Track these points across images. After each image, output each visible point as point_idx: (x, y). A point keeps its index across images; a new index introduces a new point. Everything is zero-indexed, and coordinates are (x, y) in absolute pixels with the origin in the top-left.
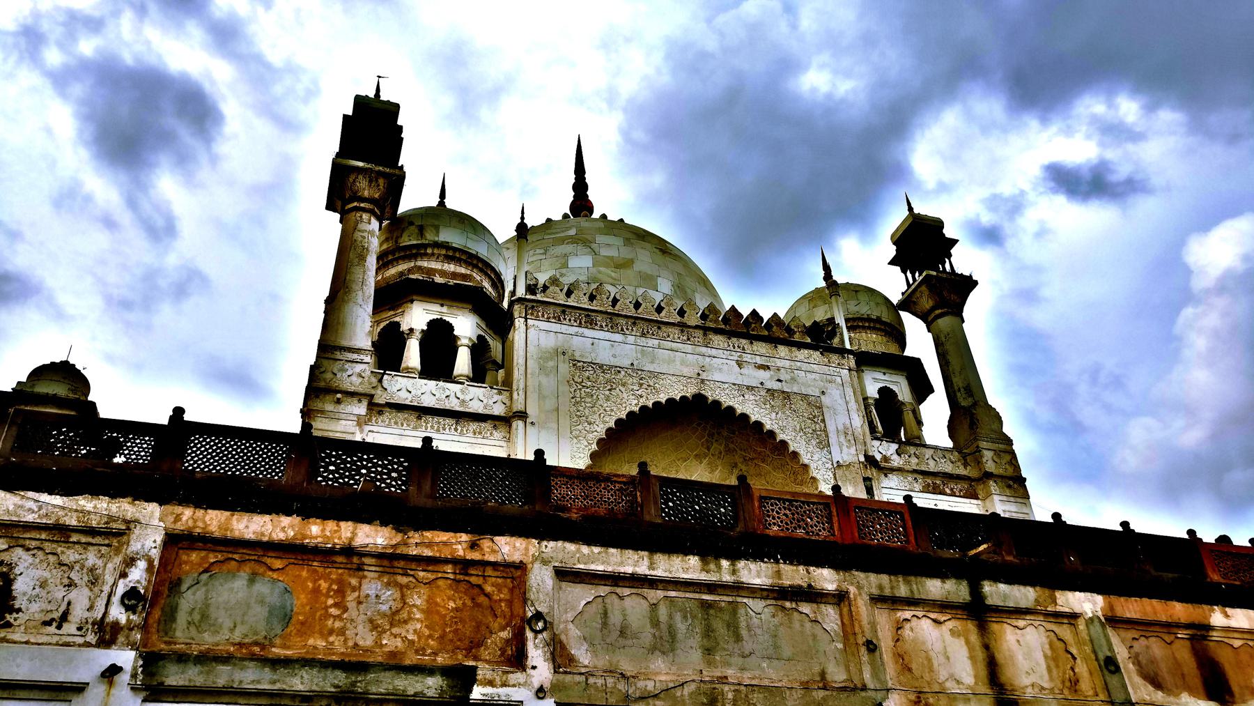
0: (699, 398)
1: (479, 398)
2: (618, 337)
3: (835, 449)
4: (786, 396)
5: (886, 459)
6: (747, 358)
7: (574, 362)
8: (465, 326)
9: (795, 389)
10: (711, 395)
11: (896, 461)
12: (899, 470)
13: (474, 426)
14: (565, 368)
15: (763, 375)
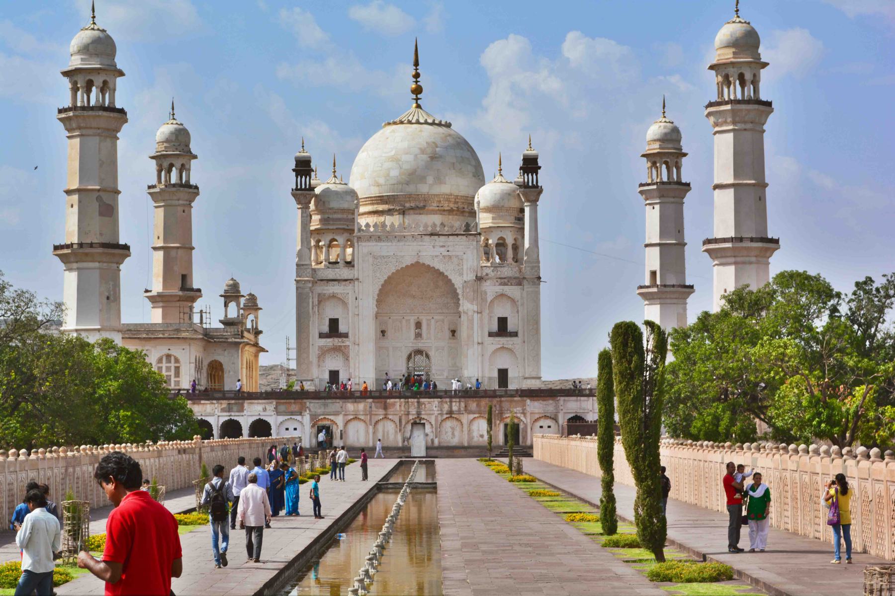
0: (418, 263)
1: (345, 273)
2: (390, 244)
3: (465, 276)
4: (450, 257)
5: (487, 275)
6: (437, 244)
7: (375, 257)
8: (341, 240)
9: (454, 253)
10: (421, 261)
11: (492, 274)
12: (490, 278)
13: (344, 283)
14: (371, 260)
15: (442, 249)
